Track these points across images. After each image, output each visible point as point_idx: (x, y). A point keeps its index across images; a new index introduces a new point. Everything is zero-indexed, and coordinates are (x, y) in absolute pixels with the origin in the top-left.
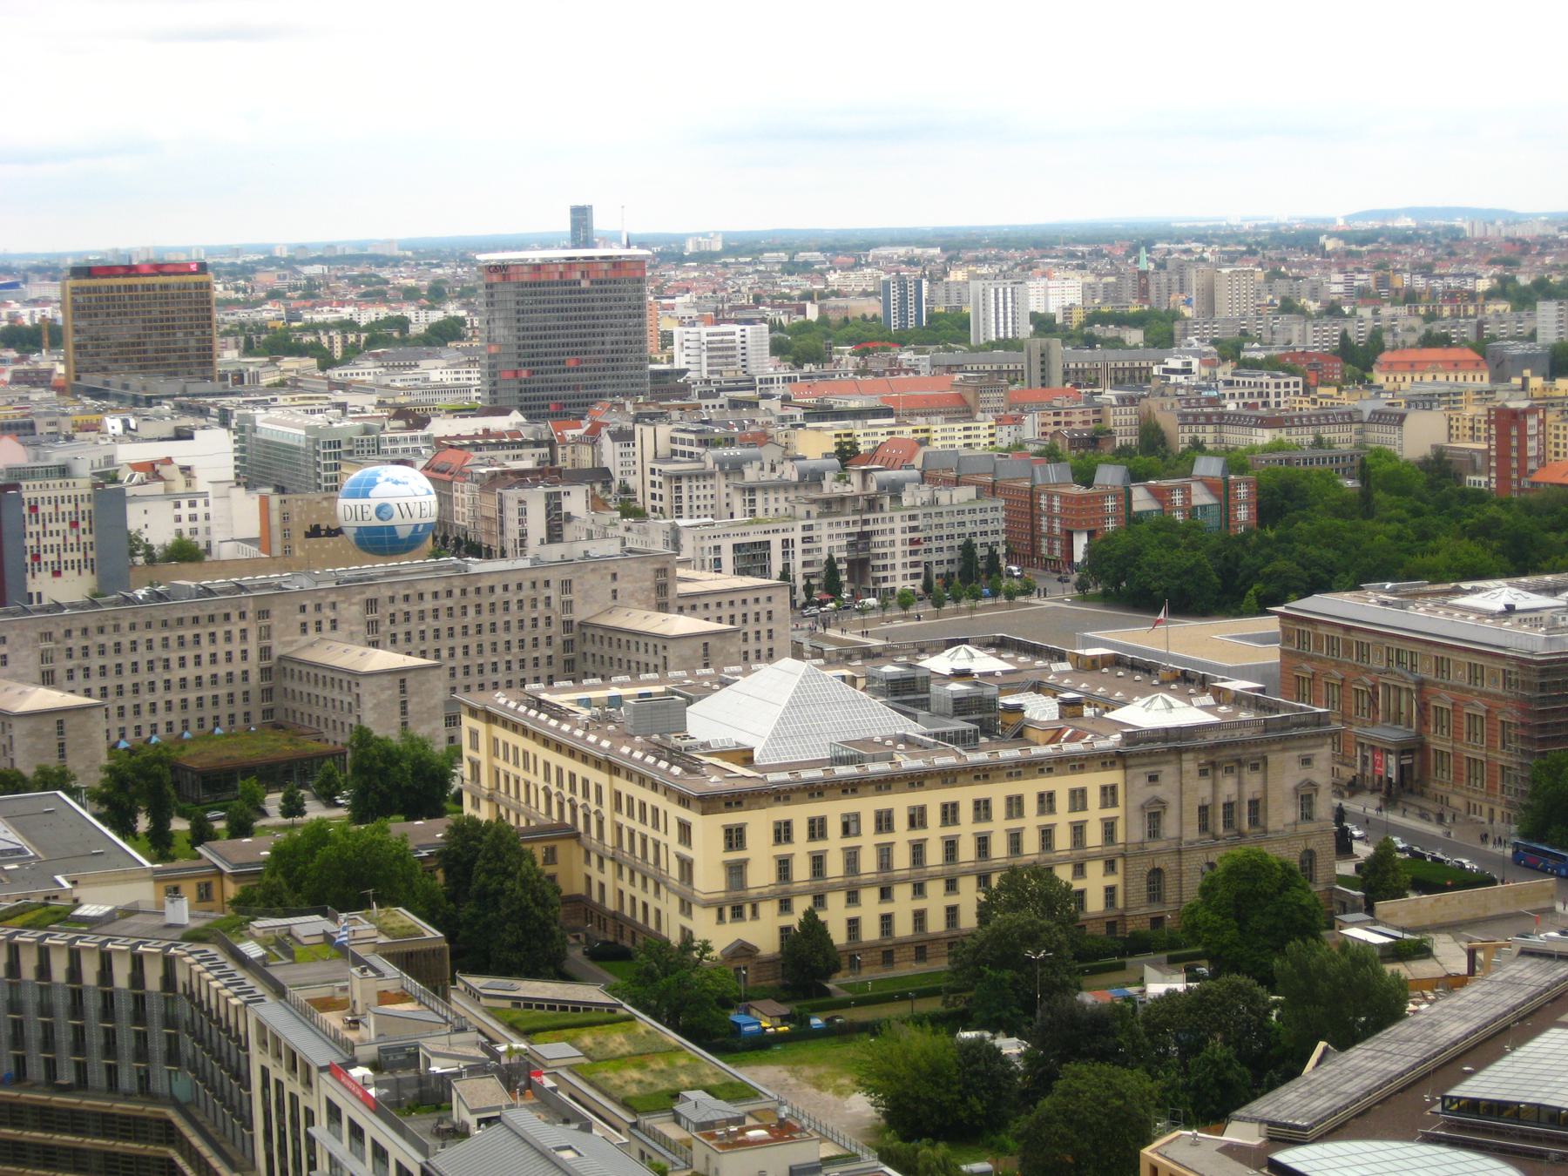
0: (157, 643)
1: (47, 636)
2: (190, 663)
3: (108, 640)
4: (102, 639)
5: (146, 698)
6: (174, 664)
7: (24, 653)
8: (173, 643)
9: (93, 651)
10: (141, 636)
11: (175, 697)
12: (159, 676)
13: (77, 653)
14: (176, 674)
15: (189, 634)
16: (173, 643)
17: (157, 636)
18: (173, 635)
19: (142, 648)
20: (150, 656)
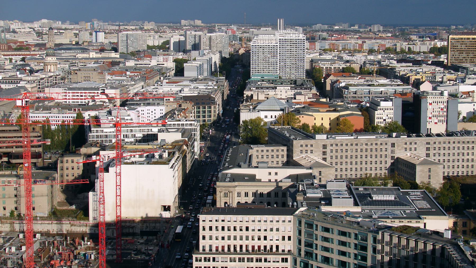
0: (461, 148)
1: (428, 143)
2: (470, 154)
3: (447, 146)
4: (444, 145)
5: (456, 164)
6: (465, 154)
7: (421, 147)
8: (466, 148)
9: (442, 149)
10: (456, 145)
11: (465, 164)
12: (461, 157)
13: (437, 149)
14: (466, 157)
15: (470, 146)
16: (466, 148)
17: (461, 146)
18: (466, 146)
19: (456, 149)
20: (459, 151)
